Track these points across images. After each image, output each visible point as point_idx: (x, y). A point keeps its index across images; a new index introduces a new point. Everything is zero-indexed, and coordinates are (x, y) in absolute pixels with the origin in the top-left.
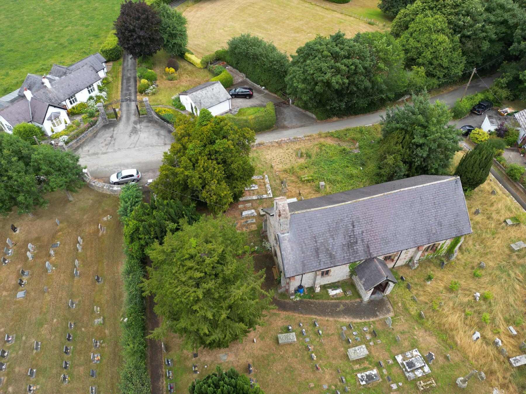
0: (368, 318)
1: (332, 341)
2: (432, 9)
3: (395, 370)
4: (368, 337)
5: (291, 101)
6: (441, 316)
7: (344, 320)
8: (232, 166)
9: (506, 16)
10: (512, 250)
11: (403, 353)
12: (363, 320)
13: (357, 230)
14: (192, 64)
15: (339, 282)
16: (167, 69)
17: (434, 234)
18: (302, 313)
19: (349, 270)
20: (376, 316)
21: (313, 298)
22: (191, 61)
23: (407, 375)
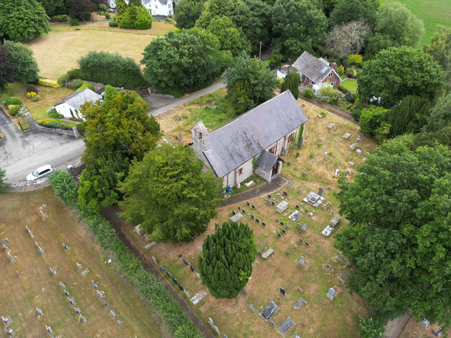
0: (276, 189)
1: (264, 209)
2: (218, 14)
3: (307, 207)
4: (282, 197)
5: (150, 91)
6: (314, 171)
7: (264, 196)
8: (146, 121)
9: (263, 10)
10: (329, 129)
12: (274, 191)
13: (249, 136)
14: (49, 86)
15: (248, 178)
16: (29, 94)
17: (290, 126)
18: (236, 203)
19: (252, 166)
20: (280, 186)
21: (238, 192)
22: (47, 85)
23: (314, 205)
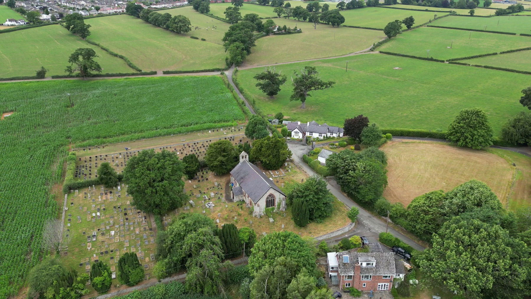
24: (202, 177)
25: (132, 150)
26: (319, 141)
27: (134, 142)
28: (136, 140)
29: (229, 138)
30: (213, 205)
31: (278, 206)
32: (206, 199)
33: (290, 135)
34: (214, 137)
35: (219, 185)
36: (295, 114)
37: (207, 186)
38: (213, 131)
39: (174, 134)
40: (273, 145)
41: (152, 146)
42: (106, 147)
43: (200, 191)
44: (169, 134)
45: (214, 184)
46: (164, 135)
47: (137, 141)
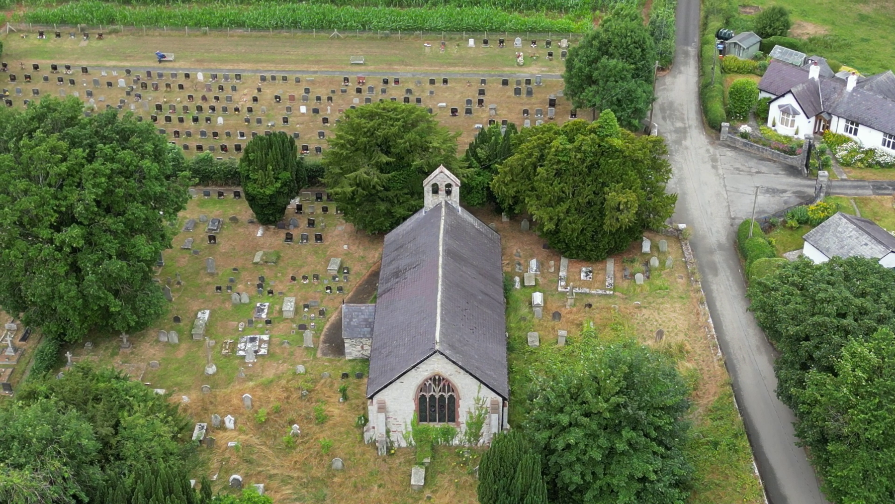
0: (326, 335)
7: (334, 316)
11: (269, 342)
12: (325, 330)
18: (360, 286)
20: (325, 342)
24: (311, 223)
25: (176, 65)
26: (870, 166)
27: (205, 34)
28: (215, 27)
29: (518, 83)
30: (263, 351)
31: (469, 425)
32: (259, 318)
33: (762, 115)
34: (475, 65)
35: (341, 268)
36: (863, 18)
37: (301, 267)
38: (486, 42)
39: (345, 29)
40: (583, 161)
41: (248, 62)
42: (113, 36)
43: (262, 279)
44: (323, 25)
45: (328, 261)
46: (309, 28)
47: (215, 33)
